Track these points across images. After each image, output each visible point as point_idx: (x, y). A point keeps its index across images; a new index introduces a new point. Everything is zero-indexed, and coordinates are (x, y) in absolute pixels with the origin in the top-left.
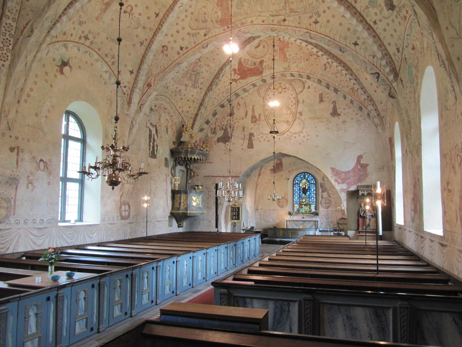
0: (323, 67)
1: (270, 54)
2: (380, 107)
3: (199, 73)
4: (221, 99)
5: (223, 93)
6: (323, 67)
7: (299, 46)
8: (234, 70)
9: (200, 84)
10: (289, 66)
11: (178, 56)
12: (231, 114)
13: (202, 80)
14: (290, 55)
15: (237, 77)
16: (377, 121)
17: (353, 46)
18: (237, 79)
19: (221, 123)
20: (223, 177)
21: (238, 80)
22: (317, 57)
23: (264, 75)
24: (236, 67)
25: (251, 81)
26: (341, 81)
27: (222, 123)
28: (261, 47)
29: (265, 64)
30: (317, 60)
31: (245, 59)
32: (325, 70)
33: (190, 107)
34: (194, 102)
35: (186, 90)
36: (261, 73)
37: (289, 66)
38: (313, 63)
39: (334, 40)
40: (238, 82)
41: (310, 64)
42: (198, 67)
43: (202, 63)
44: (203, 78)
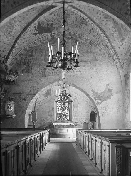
1: (58, 20)
2: (120, 58)
3: (13, 26)
4: (25, 45)
5: (26, 41)
7: (76, 17)
9: (13, 34)
10: (68, 29)
11: (11, 8)
12: (31, 56)
13: (15, 31)
14: (70, 22)
16: (118, 64)
17: (125, 15)
19: (24, 61)
20: (26, 94)
23: (53, 33)
24: (37, 26)
26: (99, 41)
27: (25, 60)
28: (53, 15)
29: (54, 26)
30: (86, 27)
31: (42, 22)
32: (90, 33)
33: (5, 48)
34: (8, 45)
35: (4, 36)
36: (51, 31)
37: (68, 29)
38: (83, 28)
39: (114, 10)
42: (13, 22)
43: (16, 19)
44: (16, 29)
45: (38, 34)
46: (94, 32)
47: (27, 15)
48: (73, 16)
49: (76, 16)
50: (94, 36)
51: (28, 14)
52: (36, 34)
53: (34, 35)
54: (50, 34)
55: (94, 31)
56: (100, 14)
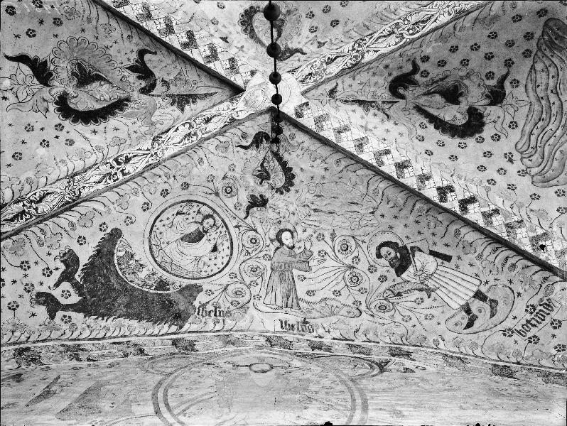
0: (458, 318)
6: (458, 318)
8: (70, 260)
10: (305, 322)
15: (66, 294)
18: (63, 301)
22: (424, 295)
24: (85, 255)
25: (125, 331)
28: (204, 246)
29: (201, 298)
30: (428, 302)
32: (470, 325)
36: (180, 318)
37: (305, 322)
40: (60, 314)
41: (398, 318)
46: (502, 308)
47: (45, 143)
48: (330, 263)
49: (348, 261)
50: (508, 332)
51: (53, 142)
52: (58, 303)
53: (42, 310)
54: (165, 328)
56: (501, 171)
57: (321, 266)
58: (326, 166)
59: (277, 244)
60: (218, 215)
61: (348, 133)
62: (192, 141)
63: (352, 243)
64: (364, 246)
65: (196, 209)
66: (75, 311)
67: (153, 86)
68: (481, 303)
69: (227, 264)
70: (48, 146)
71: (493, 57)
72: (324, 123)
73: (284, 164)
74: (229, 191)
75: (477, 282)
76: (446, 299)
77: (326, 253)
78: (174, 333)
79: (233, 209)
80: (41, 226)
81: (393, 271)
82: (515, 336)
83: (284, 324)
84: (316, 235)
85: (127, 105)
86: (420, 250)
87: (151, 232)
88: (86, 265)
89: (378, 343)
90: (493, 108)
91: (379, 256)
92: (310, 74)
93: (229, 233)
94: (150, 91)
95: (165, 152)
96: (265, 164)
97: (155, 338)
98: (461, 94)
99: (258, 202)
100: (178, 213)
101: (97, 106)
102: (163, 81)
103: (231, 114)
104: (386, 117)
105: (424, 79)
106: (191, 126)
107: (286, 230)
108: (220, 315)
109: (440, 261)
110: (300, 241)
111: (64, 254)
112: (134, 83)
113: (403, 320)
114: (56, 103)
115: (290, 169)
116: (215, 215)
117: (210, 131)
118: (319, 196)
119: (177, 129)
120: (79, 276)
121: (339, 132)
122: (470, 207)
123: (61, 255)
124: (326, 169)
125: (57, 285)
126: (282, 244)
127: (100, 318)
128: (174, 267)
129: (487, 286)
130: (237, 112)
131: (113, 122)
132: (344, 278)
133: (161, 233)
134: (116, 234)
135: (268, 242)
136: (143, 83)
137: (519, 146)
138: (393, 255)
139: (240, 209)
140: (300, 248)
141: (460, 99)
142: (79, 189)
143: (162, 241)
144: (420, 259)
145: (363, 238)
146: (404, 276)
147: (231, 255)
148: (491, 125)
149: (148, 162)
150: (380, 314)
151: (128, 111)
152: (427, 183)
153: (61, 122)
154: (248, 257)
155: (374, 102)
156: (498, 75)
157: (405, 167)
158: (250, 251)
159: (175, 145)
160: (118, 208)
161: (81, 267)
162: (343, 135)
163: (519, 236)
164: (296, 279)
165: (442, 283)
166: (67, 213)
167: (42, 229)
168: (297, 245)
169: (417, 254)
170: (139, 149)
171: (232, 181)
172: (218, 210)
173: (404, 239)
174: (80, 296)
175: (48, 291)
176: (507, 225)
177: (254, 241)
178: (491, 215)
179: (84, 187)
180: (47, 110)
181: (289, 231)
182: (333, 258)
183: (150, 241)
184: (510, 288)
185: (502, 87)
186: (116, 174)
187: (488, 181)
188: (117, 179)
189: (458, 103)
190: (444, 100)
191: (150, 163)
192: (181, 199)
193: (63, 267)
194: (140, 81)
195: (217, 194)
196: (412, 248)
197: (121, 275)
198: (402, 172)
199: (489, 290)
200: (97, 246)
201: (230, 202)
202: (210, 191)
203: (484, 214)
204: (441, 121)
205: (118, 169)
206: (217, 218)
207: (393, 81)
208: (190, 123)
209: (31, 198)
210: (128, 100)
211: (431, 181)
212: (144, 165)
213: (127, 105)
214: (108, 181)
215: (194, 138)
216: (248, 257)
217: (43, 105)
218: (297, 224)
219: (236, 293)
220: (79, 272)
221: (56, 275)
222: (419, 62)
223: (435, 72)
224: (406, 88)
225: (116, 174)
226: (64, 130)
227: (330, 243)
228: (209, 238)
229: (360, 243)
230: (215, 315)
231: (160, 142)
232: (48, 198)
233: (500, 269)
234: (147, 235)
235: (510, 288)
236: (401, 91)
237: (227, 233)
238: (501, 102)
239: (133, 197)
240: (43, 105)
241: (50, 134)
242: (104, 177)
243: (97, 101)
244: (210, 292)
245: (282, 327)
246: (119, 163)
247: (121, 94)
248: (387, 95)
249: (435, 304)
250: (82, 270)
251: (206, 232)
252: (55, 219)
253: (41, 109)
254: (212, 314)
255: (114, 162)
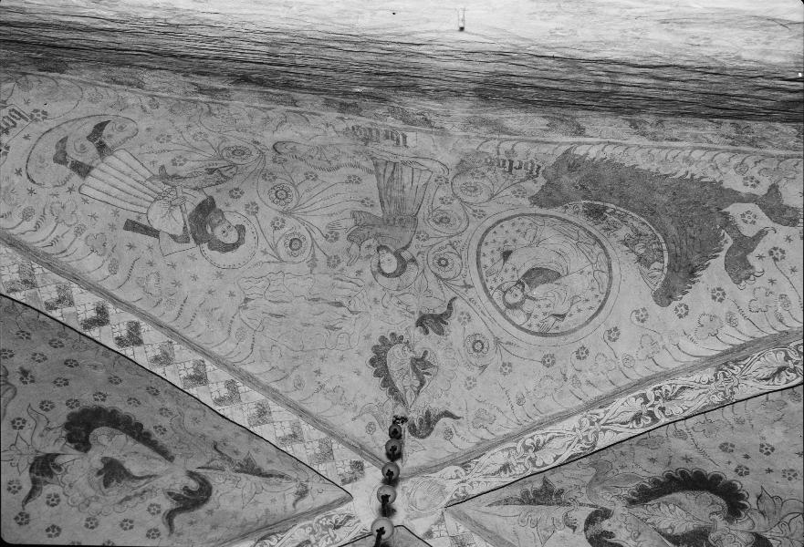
7: (288, 213)
21: (752, 199)
29: (534, 187)
40: (761, 190)
45: (739, 198)
47: (767, 450)
49: (290, 222)
51: (754, 451)
52: (763, 207)
55: (61, 158)
57: (334, 218)
58: (318, 379)
59: (406, 255)
60: (498, 307)
61: (280, 434)
62: (532, 438)
63: (283, 251)
64: (263, 245)
65: (534, 321)
66: (736, 193)
67: (590, 521)
68: (80, 160)
69: (487, 232)
70: (762, 446)
71: (48, 530)
72: (318, 451)
73: (388, 383)
74: (477, 345)
75: (86, 190)
76: (136, 164)
77: (326, 237)
78: (580, 144)
79: (471, 312)
80: (781, 327)
81: (219, 206)
82: (27, 110)
83: (399, 141)
84: (340, 266)
85: (633, 494)
86: (174, 237)
87: (608, 294)
88: (716, 257)
89: (247, 106)
90: (49, 450)
91: (241, 229)
92: (337, 527)
93: (481, 278)
94: (596, 513)
95: (577, 425)
96: (417, 383)
97: (612, 140)
98: (99, 473)
99: (433, 322)
100: (563, 316)
101: (679, 496)
102: (574, 528)
103: (467, 474)
104: (219, 447)
105: (154, 500)
106: (533, 461)
107: (388, 275)
108: (504, 161)
109: (145, 223)
110: (369, 256)
111: (748, 278)
112: (620, 527)
113: (206, 135)
114: (744, 507)
115: (377, 374)
116: (503, 308)
117: (503, 451)
118: (333, 328)
119: (555, 459)
120: (726, 242)
121: (294, 436)
122: (92, 314)
123: (752, 277)
124: (318, 372)
125: (762, 234)
126: (397, 255)
127: (697, 177)
128: (575, 235)
129: (69, 184)
130: (458, 477)
131: (658, 471)
132: (299, 199)
133: (593, 289)
134: (666, 295)
135: (419, 259)
136: (605, 525)
137: (9, 394)
138: (218, 231)
139: (462, 313)
140: (369, 246)
141: (101, 466)
142: (717, 380)
143: (591, 277)
144: (174, 223)
145: (265, 259)
146: (200, 198)
147: (480, 245)
148: (54, 424)
149: (606, 412)
150: (246, 145)
151: (632, 486)
152: (158, 353)
153: (740, 479)
154: (453, 239)
155: (237, 471)
156: (41, 499)
157: (191, 378)
158: (450, 248)
159: (561, 436)
160: (657, 338)
161: (723, 254)
162: (289, 431)
163: (15, 269)
164: (377, 201)
165: (141, 187)
166: (738, 342)
167: (781, 321)
168: (372, 251)
169: (179, 232)
170: (618, 433)
171: (473, 360)
172: (499, 317)
173: (198, 255)
174: (726, 214)
175: (776, 225)
176: (33, 285)
177: (443, 263)
178: (59, 301)
179: (709, 383)
180: (759, 497)
181: (383, 274)
182: (316, 230)
183: (611, 278)
184: (33, 181)
185: (34, 481)
186: (657, 398)
187: (62, 346)
188: (655, 389)
189: (104, 460)
190: (126, 466)
191: (602, 410)
192: (554, 339)
193: (751, 258)
194: (609, 529)
195: (497, 341)
196: (187, 241)
197: (659, 235)
198: (196, 370)
199: (68, 179)
200: (694, 283)
201: (477, 325)
202: (508, 347)
203: (71, 303)
204: (132, 435)
205: (653, 406)
206: (500, 303)
207: (205, 501)
208: (535, 466)
209: (794, 375)
210: (632, 503)
211: (151, 355)
212: (612, 408)
213: (633, 494)
214: (669, 388)
215: (529, 442)
216: (453, 239)
217: (768, 505)
218: (371, 285)
219: (476, 189)
220: (727, 247)
221: (761, 248)
222: (163, 529)
223: (138, 511)
224: (186, 489)
225: (657, 398)
226: (733, 466)
227: (318, 253)
228: (515, 273)
229: (270, 251)
230: (511, 162)
231: (584, 441)
232: (766, 372)
233: (47, 211)
234: (614, 290)
235: (33, 181)
236: (193, 485)
237: (485, 278)
238: (37, 459)
239: (633, 352)
240: (768, 505)
241: (756, 464)
242: (676, 395)
243: (680, 504)
244: (520, 193)
245: (405, 137)
246: (651, 414)
247: (640, 511)
248: (216, 480)
249: (153, 157)
250: (720, 251)
251: (519, 282)
252: (759, 335)
253: (768, 501)
254: (516, 164)
255: (658, 417)
